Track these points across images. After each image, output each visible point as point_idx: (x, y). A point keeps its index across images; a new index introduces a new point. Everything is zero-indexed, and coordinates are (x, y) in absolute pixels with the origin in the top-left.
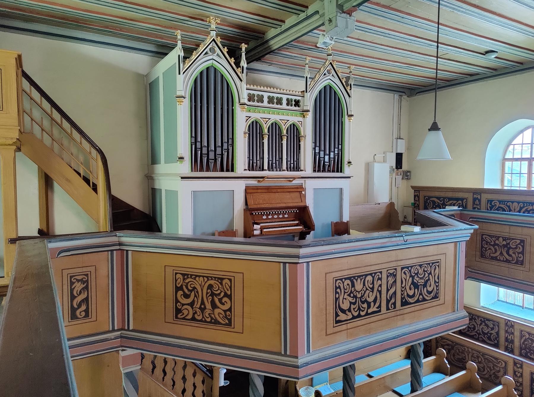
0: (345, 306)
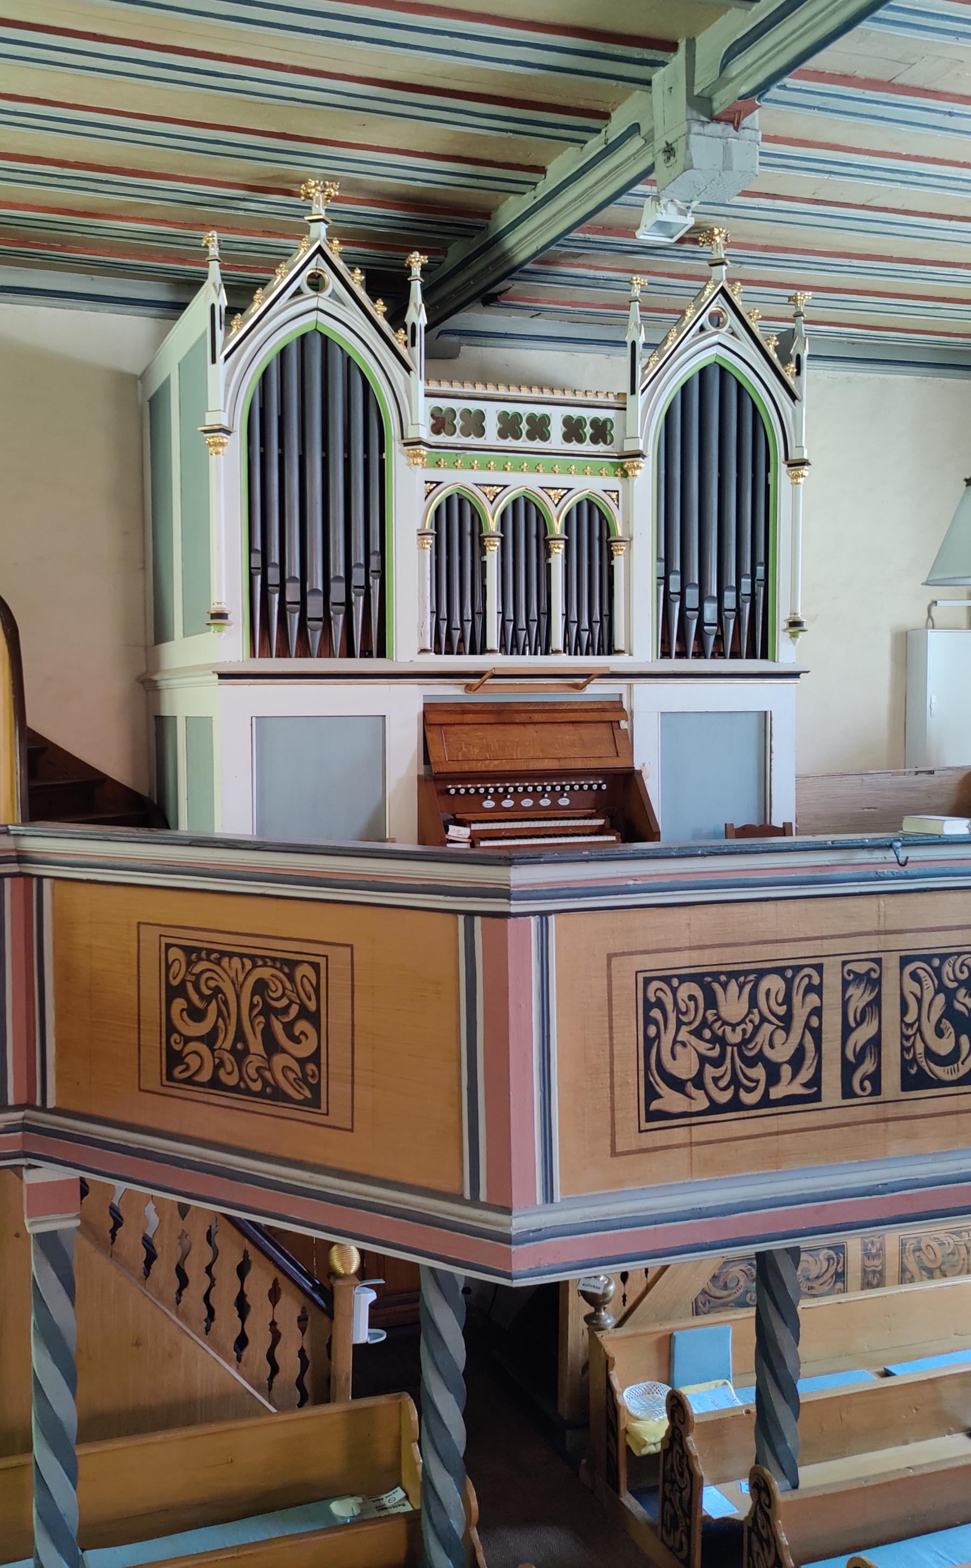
0: (684, 1066)
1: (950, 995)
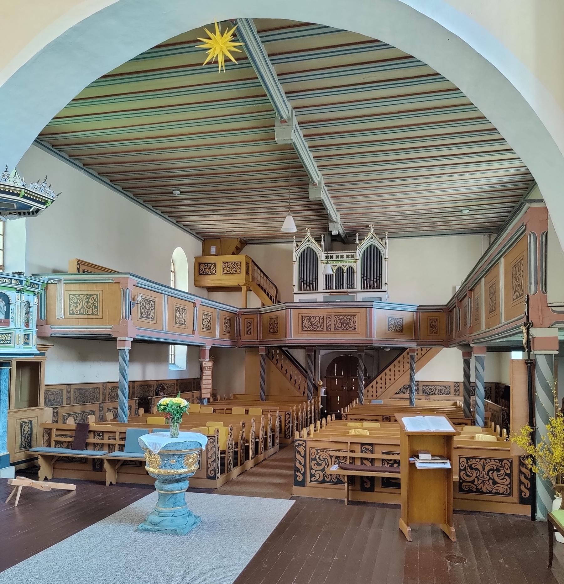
0: (307, 325)
1: (341, 320)
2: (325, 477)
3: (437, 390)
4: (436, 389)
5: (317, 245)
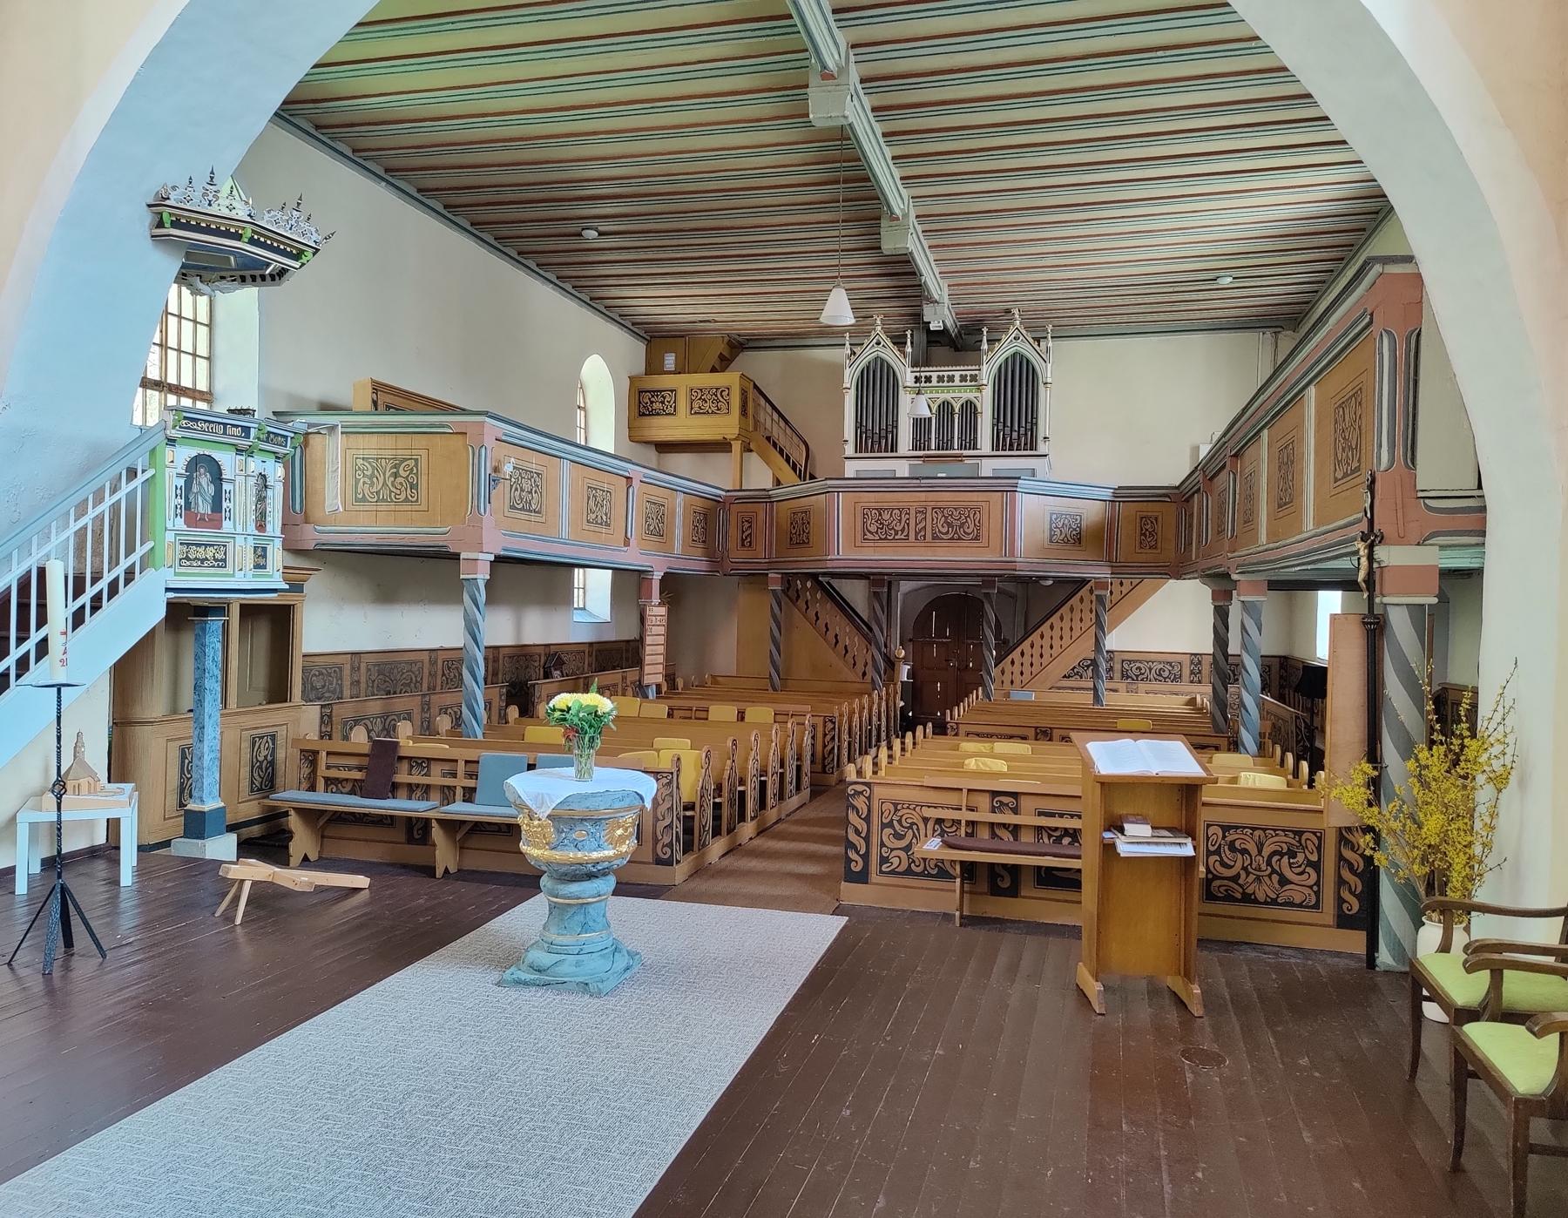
0: (873, 528)
2: (913, 865)
3: (1153, 671)
4: (1150, 669)
5: (897, 353)
